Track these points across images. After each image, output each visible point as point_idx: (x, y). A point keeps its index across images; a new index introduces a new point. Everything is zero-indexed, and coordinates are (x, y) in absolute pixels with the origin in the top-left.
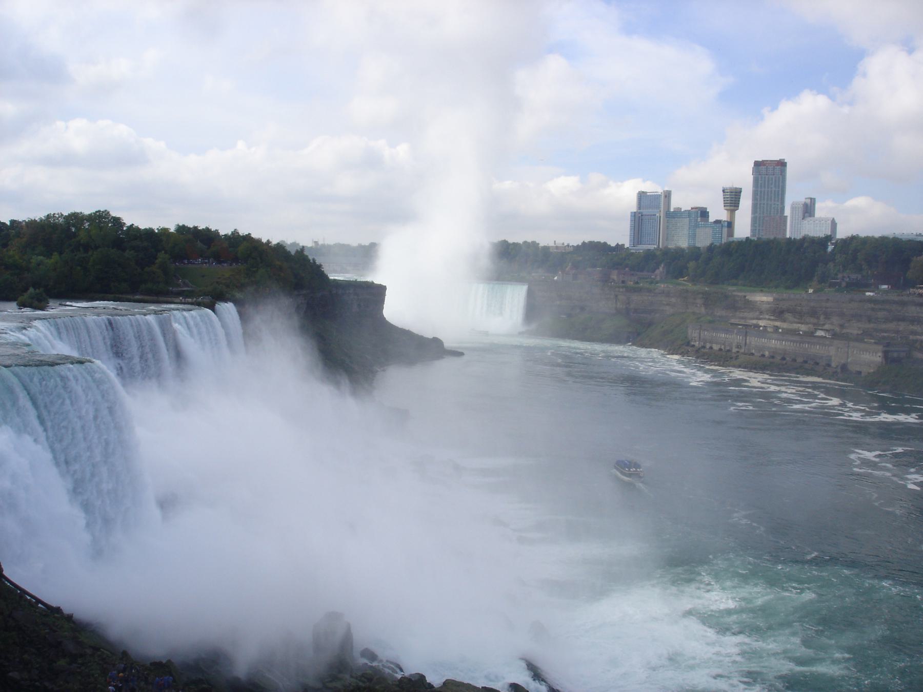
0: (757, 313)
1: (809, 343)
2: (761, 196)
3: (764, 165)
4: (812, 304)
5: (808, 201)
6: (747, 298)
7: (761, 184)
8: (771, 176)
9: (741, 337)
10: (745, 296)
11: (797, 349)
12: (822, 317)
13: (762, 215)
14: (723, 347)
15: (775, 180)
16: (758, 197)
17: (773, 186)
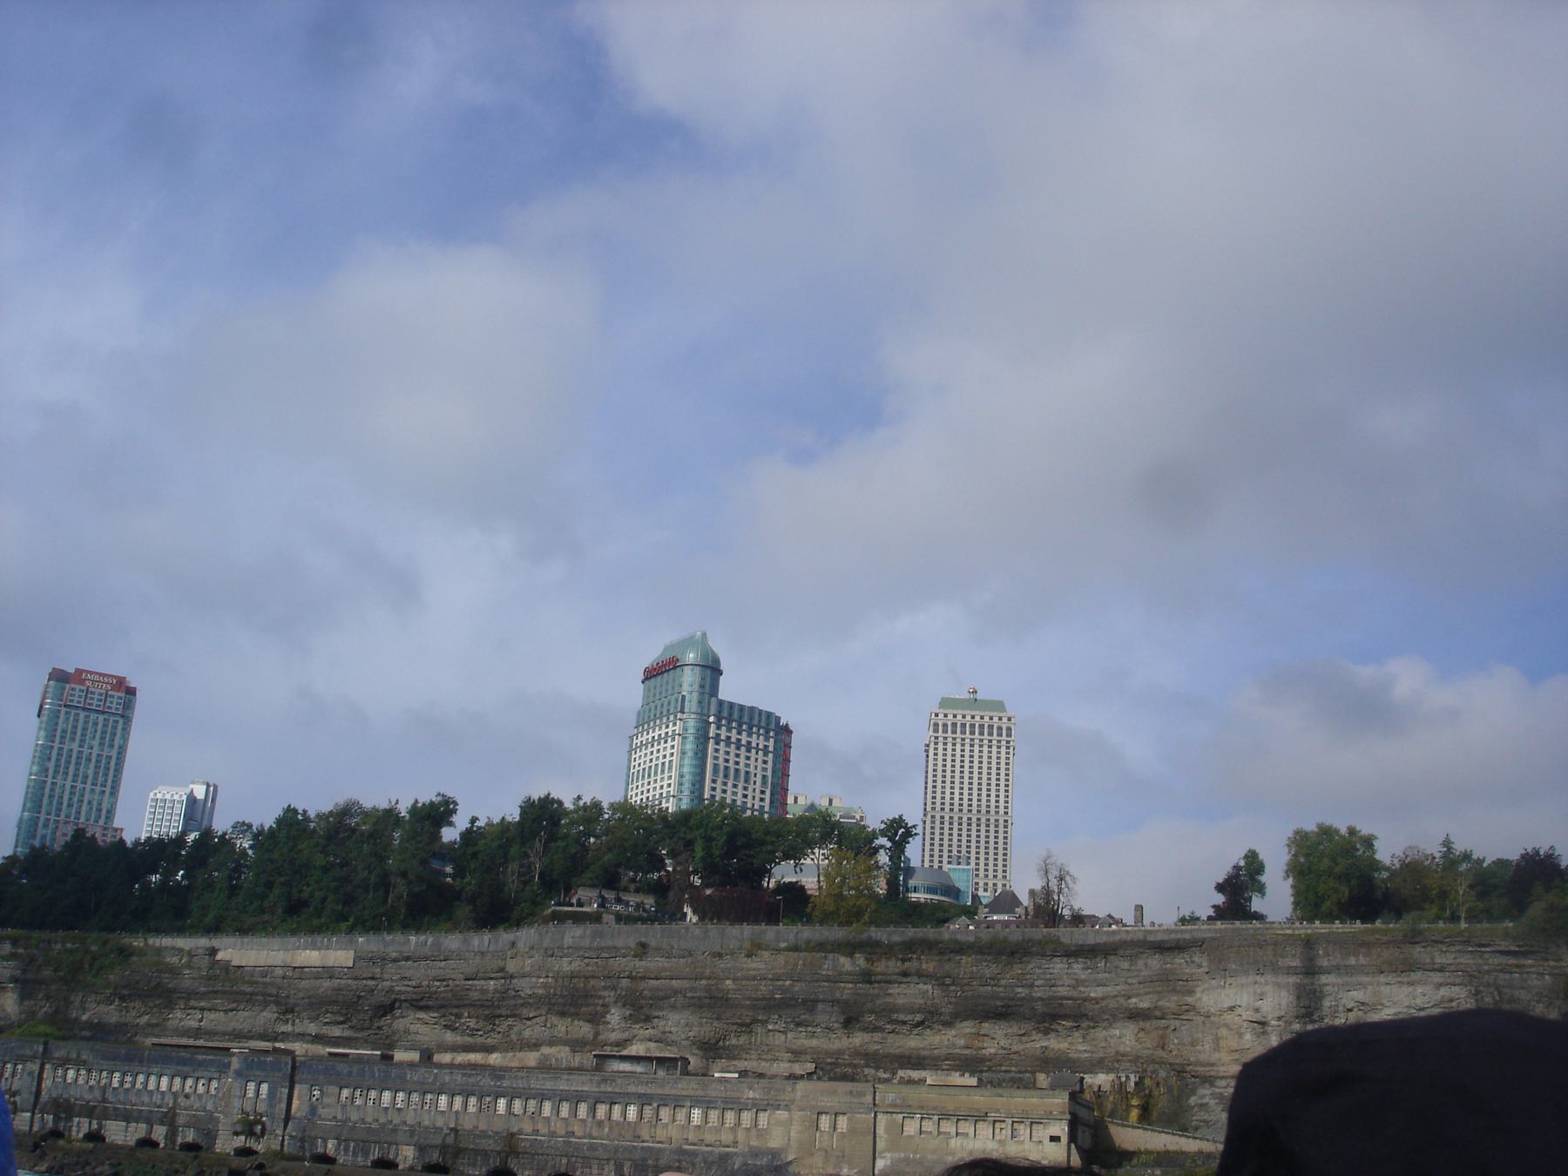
0: (269, 1014)
1: (644, 1100)
2: (58, 766)
3: (82, 682)
4: (566, 965)
5: (200, 792)
6: (219, 956)
7: (64, 731)
8: (93, 716)
9: (264, 1088)
10: (213, 952)
11: (577, 1129)
12: (615, 1017)
13: (52, 817)
14: (159, 1133)
15: (104, 732)
16: (51, 766)
17: (96, 743)
